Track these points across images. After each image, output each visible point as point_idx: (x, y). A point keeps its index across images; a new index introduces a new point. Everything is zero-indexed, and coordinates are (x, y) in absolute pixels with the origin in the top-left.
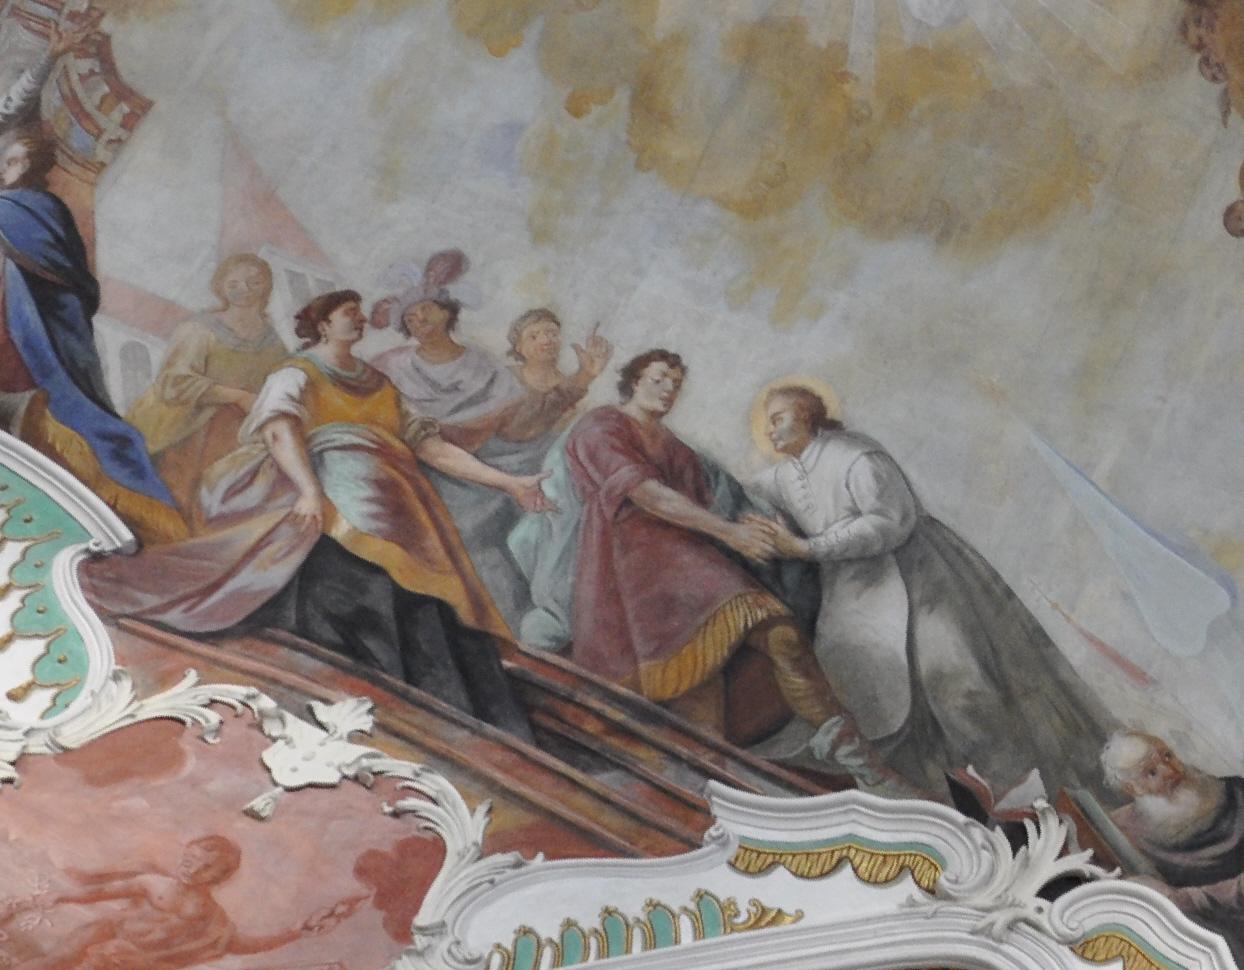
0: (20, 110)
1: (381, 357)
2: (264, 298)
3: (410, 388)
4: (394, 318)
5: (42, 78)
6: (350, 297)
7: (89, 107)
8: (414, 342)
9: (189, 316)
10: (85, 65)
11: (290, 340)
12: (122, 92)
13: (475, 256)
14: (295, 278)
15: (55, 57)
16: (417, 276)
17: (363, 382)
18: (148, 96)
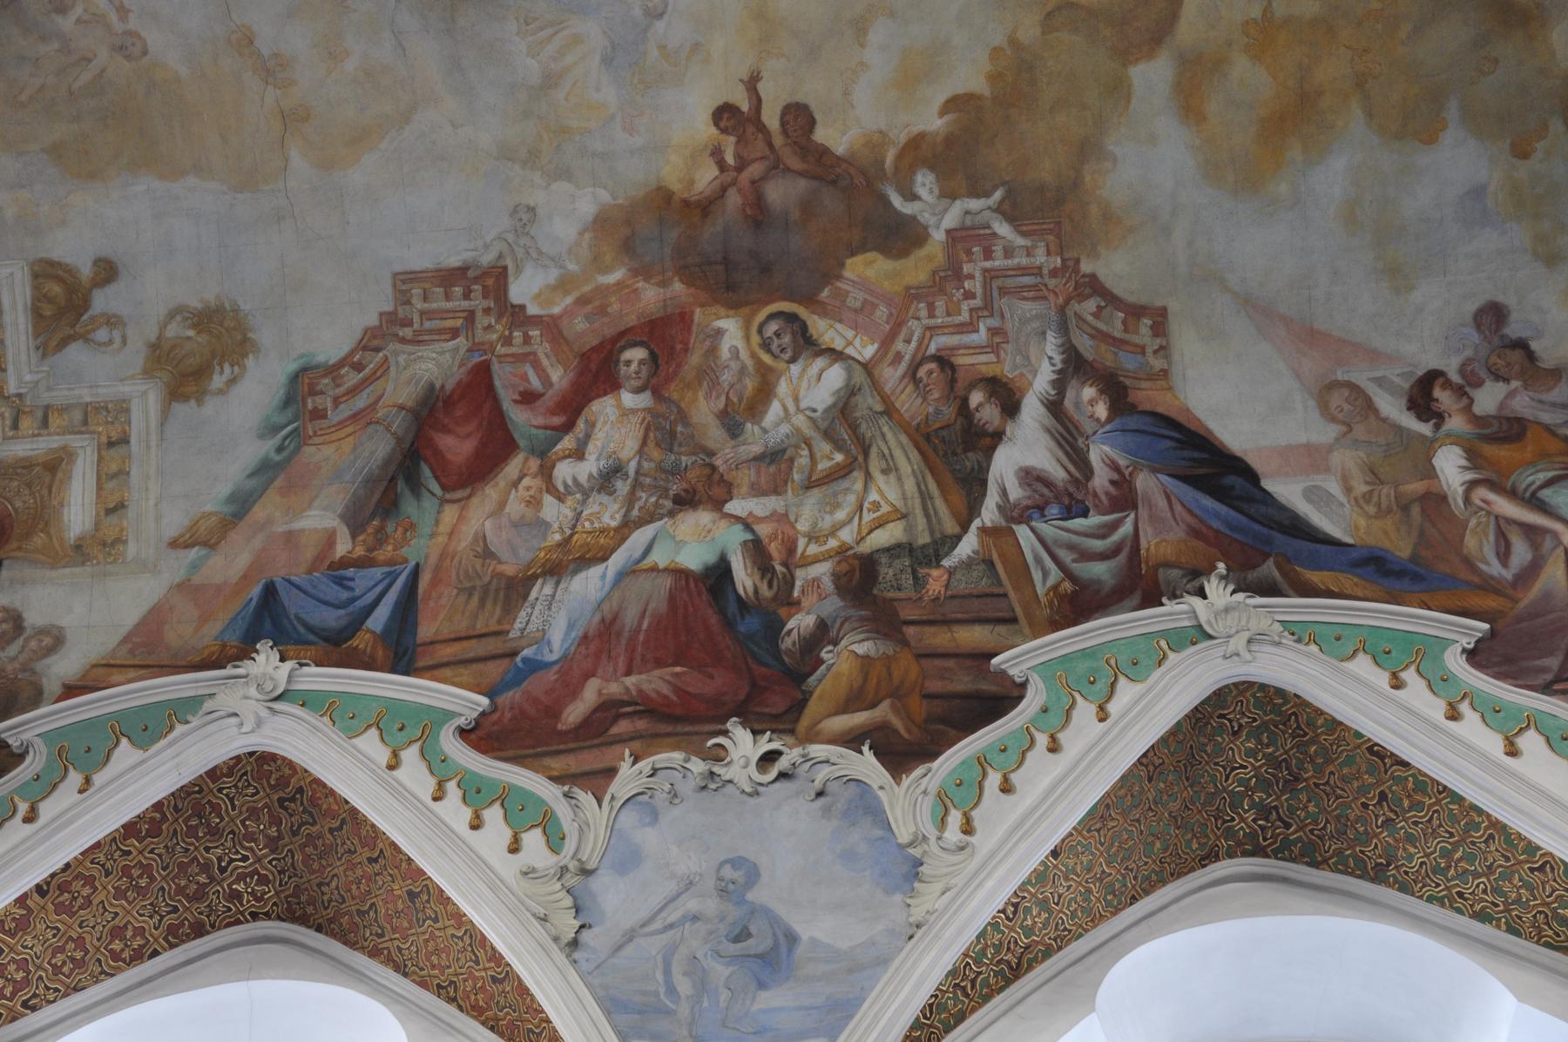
0: (1064, 362)
1: (1502, 406)
2: (1370, 406)
3: (1546, 417)
4: (1483, 374)
5: (1064, 329)
6: (1432, 378)
7: (1117, 334)
8: (1515, 384)
9: (1330, 449)
10: (1091, 305)
11: (1425, 429)
12: (1135, 312)
13: (1509, 300)
14: (1380, 382)
15: (1062, 310)
16: (1475, 337)
17: (1510, 429)
18: (1159, 303)
